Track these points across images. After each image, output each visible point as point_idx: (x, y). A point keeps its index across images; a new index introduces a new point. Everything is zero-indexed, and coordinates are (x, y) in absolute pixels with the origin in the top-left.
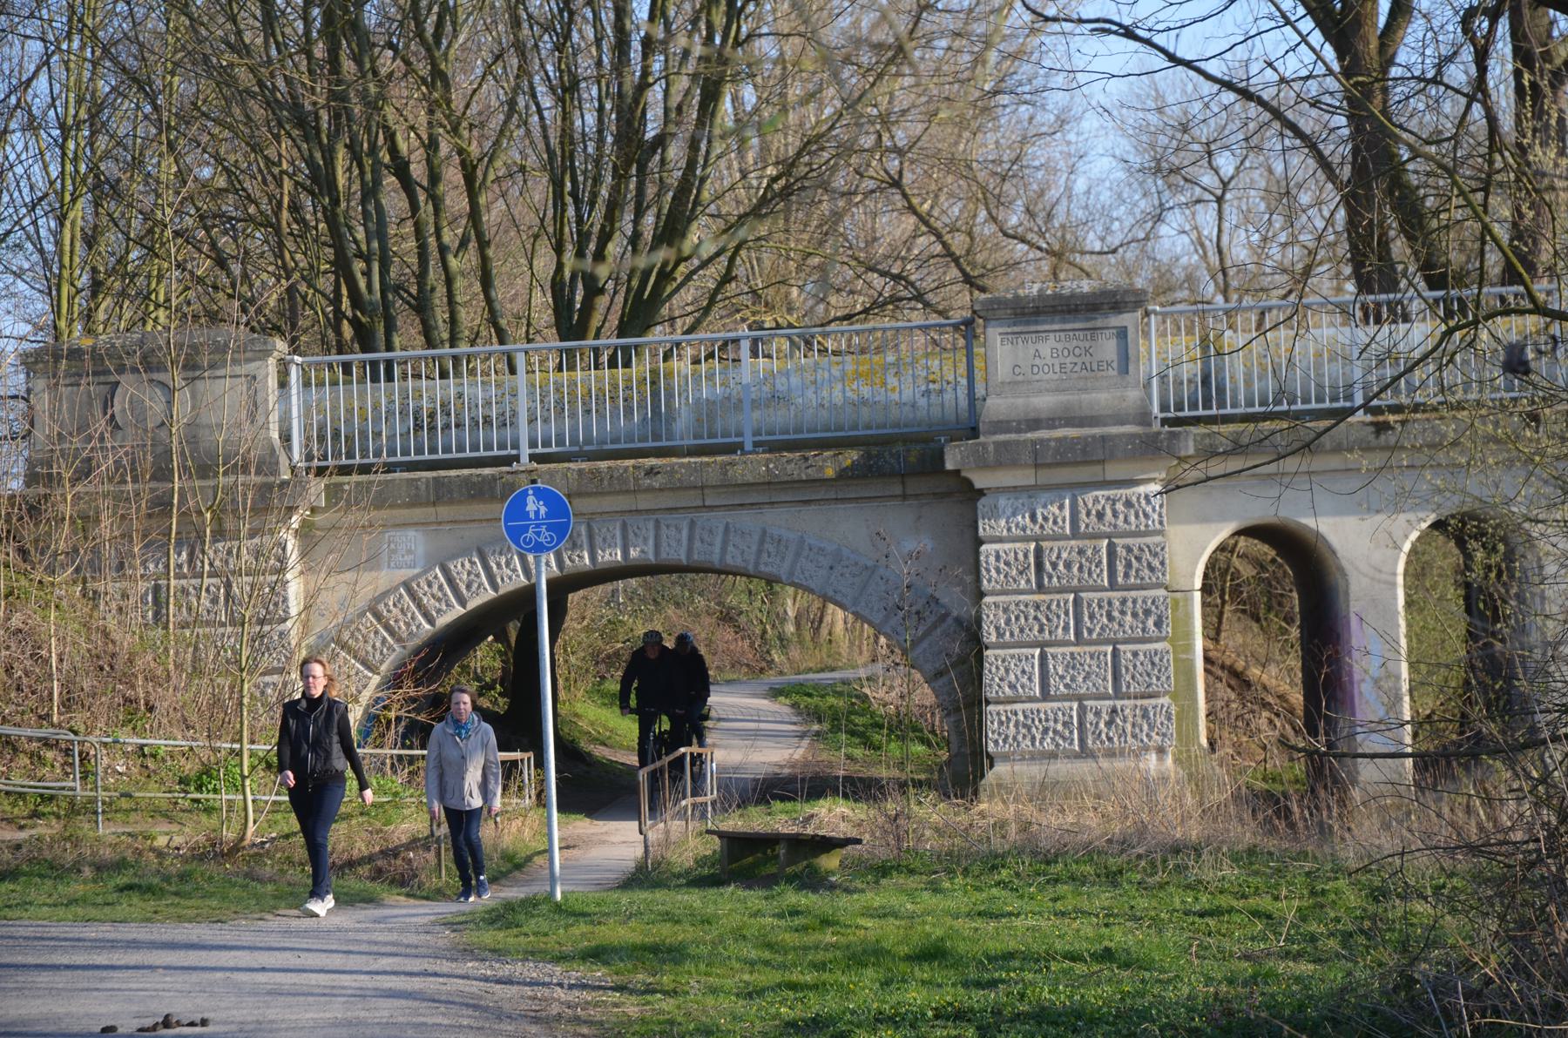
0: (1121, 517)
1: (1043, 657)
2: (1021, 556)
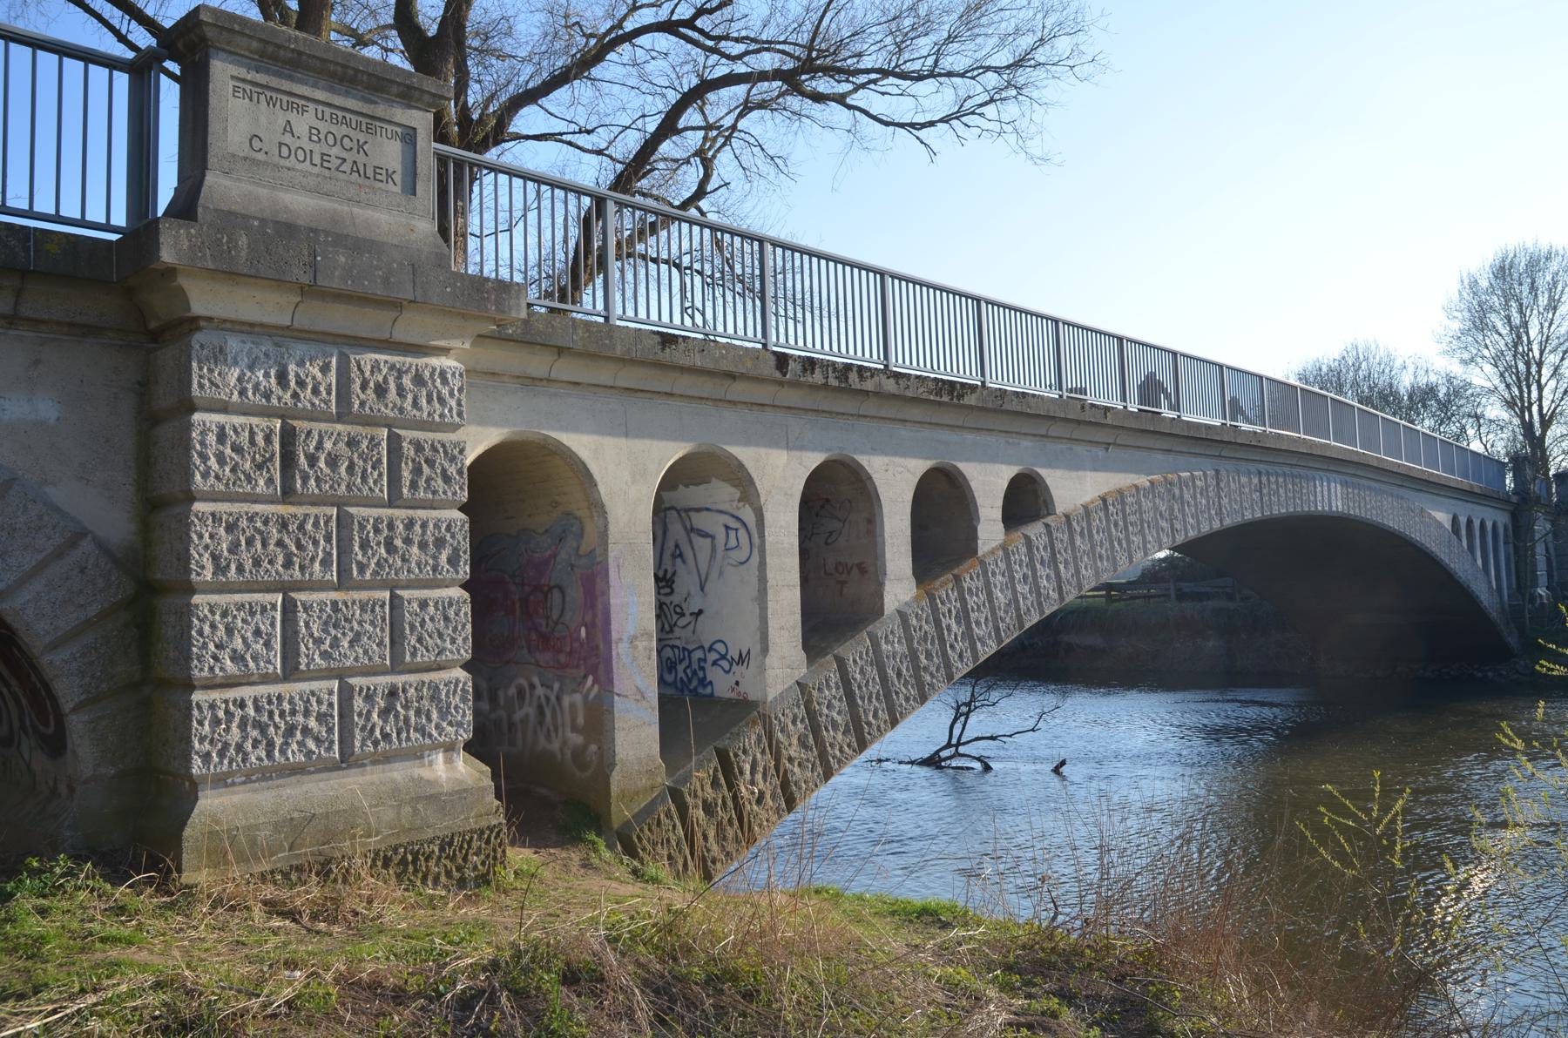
0: (410, 397)
1: (289, 609)
2: (260, 439)
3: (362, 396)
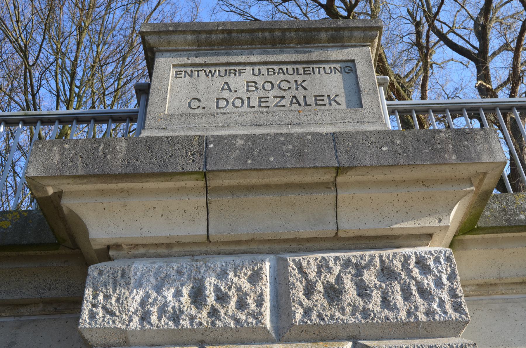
3: (307, 303)
